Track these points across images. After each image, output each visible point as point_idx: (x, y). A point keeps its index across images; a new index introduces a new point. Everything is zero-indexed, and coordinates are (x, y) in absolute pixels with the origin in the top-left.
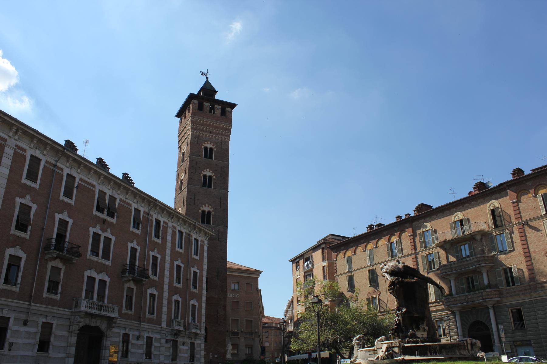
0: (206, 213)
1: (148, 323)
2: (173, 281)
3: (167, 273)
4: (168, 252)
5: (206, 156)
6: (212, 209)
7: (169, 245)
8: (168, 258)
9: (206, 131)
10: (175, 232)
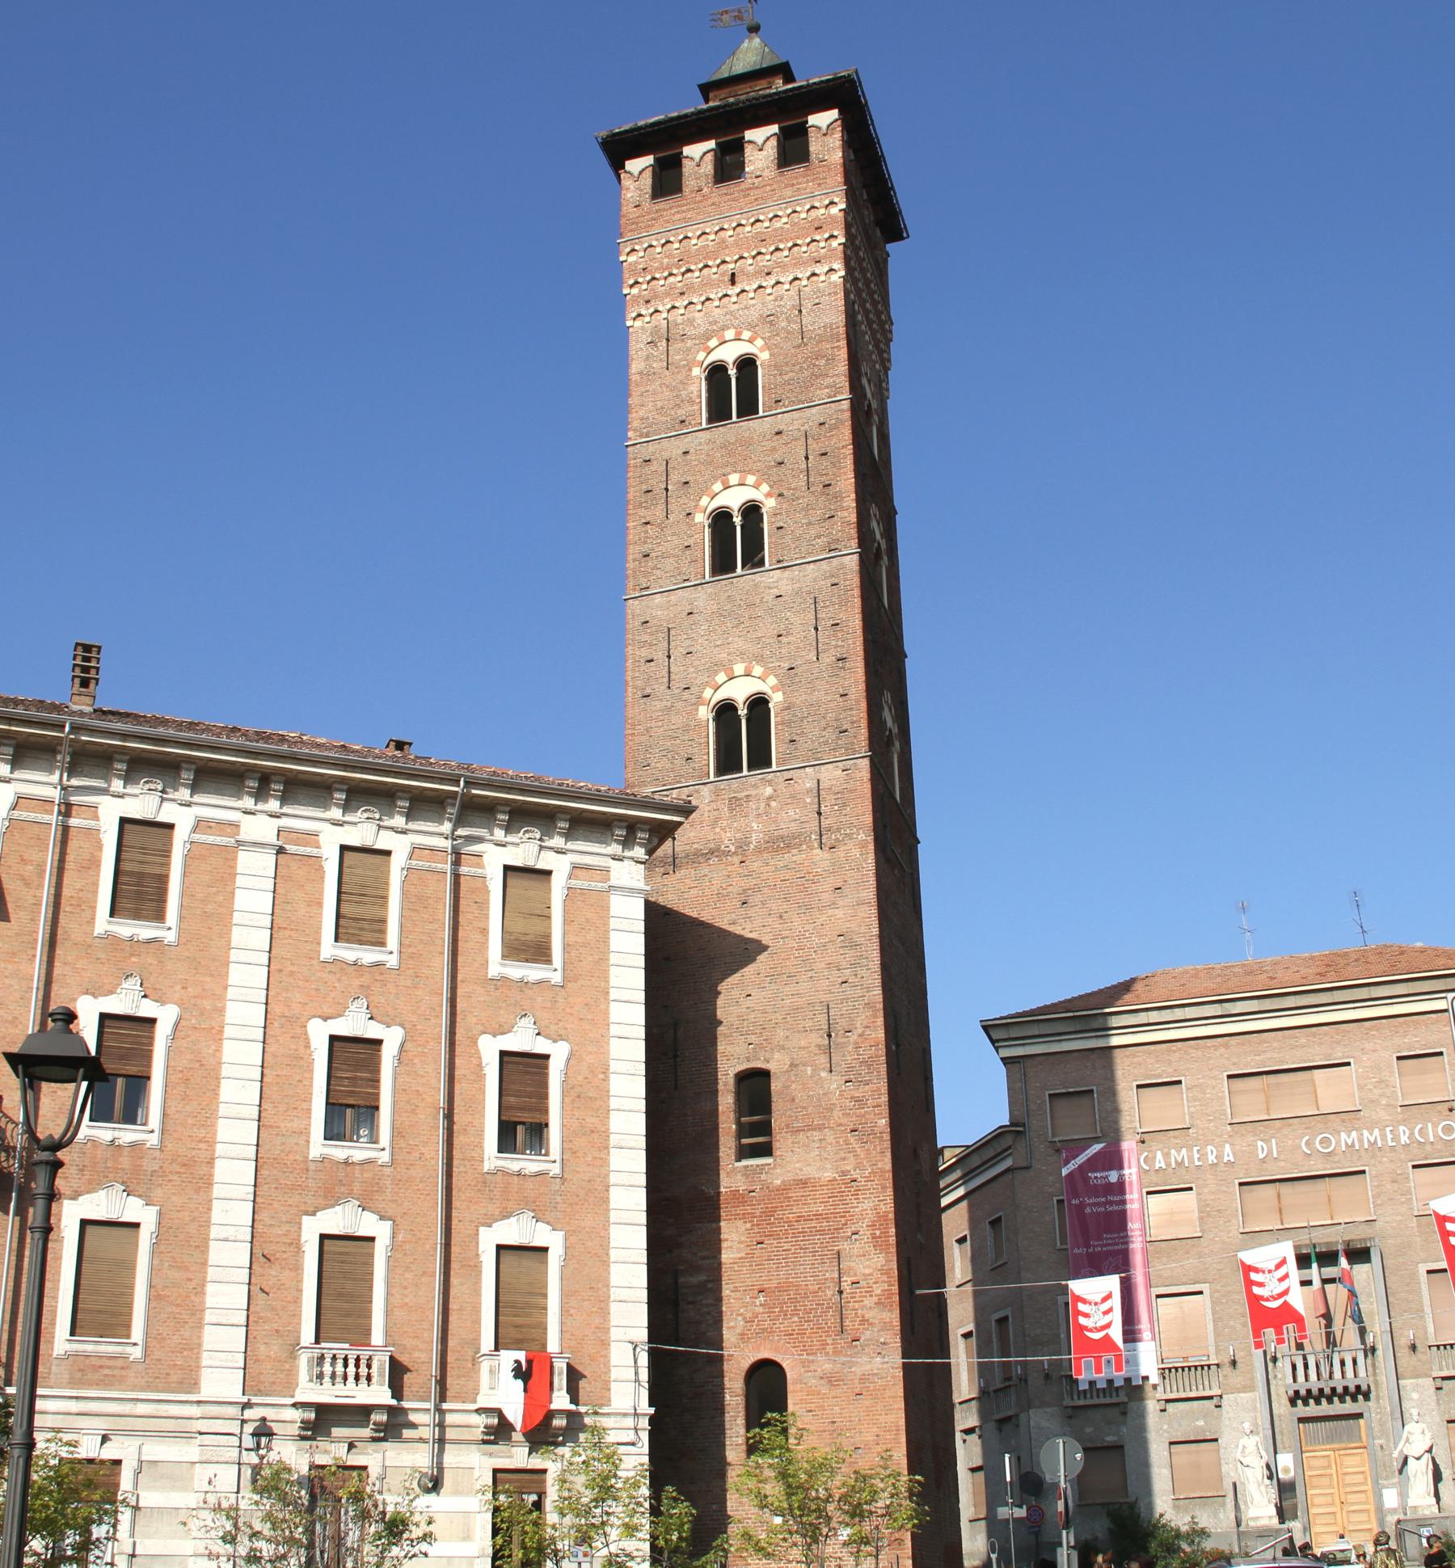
0: (743, 712)
1: (73, 1383)
2: (306, 1132)
3: (238, 1092)
4: (246, 977)
5: (718, 412)
8: (243, 1014)
9: (707, 284)
10: (314, 862)
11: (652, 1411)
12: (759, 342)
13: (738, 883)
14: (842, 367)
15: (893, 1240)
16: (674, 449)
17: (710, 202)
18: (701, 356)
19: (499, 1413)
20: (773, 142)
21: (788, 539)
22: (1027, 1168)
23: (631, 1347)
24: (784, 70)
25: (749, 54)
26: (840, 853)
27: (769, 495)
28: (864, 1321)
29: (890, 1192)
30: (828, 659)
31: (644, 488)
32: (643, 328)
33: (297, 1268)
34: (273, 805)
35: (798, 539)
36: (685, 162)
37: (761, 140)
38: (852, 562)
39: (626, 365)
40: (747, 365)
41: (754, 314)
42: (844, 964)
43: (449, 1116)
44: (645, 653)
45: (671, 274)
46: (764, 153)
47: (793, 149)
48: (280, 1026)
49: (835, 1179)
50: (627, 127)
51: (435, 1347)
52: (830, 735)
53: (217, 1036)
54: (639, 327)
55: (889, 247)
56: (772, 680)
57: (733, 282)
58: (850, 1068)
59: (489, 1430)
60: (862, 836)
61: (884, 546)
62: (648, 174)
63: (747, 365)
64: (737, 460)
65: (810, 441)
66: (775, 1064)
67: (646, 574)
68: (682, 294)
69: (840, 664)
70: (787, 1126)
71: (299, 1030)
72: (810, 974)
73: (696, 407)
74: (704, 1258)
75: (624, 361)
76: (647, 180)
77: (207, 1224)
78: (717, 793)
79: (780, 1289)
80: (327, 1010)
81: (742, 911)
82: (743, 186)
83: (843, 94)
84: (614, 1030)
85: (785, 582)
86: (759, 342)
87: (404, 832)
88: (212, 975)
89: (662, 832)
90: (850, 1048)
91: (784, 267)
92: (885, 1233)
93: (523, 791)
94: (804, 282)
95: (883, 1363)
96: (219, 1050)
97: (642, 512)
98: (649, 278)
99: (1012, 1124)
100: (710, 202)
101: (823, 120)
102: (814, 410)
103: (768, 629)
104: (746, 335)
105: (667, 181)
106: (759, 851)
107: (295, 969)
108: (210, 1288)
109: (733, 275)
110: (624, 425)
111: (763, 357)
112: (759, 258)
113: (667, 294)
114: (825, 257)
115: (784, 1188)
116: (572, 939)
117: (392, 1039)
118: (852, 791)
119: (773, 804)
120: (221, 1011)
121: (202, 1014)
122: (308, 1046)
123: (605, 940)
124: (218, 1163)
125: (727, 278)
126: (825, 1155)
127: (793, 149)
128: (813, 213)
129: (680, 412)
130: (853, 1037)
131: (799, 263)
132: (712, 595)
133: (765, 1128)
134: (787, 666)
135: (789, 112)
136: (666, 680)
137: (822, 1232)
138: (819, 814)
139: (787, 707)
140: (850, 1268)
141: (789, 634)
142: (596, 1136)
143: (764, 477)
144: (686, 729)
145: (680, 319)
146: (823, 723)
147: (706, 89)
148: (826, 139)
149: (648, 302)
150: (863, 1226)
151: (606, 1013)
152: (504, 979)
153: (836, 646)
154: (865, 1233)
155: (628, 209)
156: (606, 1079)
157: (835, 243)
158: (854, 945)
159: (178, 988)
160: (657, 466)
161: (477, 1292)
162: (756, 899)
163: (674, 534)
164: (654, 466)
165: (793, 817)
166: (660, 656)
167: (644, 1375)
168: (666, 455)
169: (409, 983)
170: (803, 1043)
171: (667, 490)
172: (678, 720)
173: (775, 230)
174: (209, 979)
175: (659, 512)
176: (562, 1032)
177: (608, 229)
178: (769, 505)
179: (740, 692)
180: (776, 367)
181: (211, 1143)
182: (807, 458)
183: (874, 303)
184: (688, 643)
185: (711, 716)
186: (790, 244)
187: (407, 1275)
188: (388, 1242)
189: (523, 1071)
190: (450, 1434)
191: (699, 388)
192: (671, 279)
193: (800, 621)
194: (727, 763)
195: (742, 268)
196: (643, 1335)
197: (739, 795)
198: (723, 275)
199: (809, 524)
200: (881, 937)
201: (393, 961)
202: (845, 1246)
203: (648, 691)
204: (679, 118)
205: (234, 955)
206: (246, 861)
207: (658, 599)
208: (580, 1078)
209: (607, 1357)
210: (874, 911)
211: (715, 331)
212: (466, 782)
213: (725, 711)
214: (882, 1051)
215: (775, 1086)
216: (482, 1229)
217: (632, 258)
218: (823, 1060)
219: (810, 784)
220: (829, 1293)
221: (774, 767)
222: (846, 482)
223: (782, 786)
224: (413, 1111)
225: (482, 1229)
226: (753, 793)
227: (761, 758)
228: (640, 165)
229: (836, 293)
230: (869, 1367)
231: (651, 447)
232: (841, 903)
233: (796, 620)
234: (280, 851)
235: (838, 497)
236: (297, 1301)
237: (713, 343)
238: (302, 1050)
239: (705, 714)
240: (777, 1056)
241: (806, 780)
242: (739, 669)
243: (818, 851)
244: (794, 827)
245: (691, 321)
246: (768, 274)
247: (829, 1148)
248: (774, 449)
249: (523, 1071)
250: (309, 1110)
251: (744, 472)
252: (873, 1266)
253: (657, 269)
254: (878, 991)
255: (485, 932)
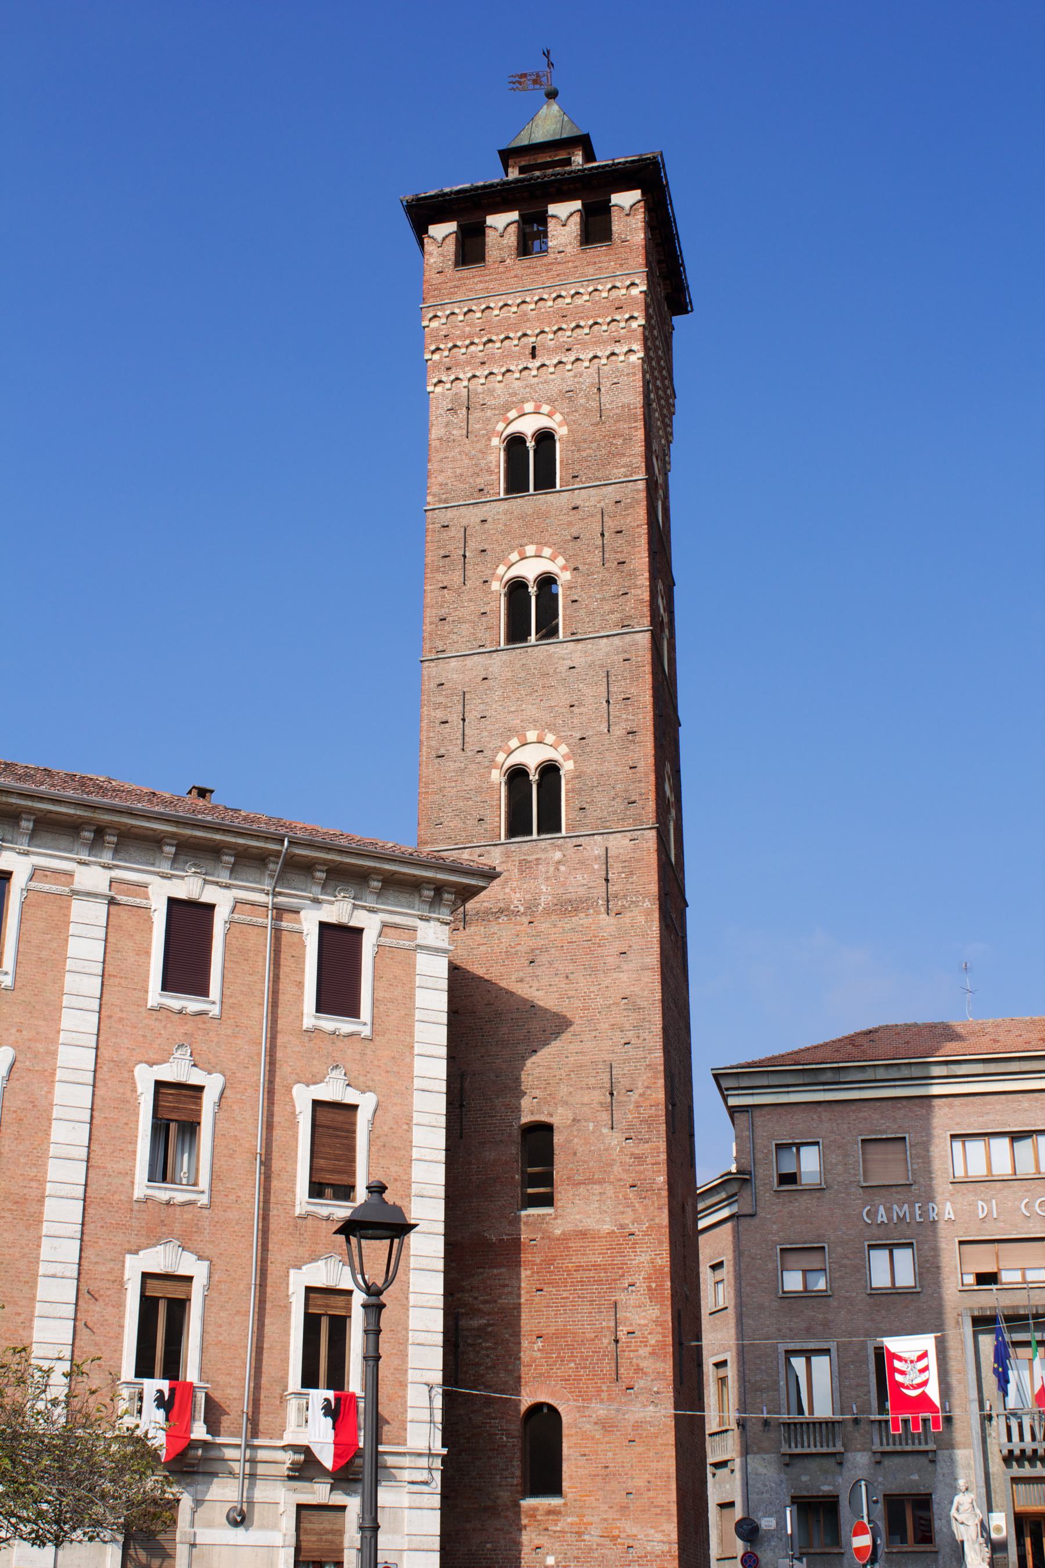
0: (534, 777)
2: (130, 1173)
3: (68, 1134)
4: (78, 1023)
5: (516, 484)
6: (564, 749)
7: (81, 985)
8: (75, 1058)
9: (508, 356)
11: (445, 1451)
12: (558, 417)
13: (526, 944)
14: (639, 448)
15: (668, 1293)
16: (472, 516)
17: (513, 273)
18: (500, 426)
19: (307, 1450)
20: (576, 219)
21: (582, 612)
22: (752, 1216)
23: (426, 1388)
24: (583, 142)
25: (547, 123)
26: (626, 919)
27: (564, 568)
28: (638, 1370)
29: (666, 1246)
30: (618, 731)
31: (442, 553)
32: (443, 394)
33: (120, 1305)
34: (107, 858)
35: (592, 613)
36: (488, 231)
37: (565, 215)
38: (644, 640)
39: (426, 429)
40: (545, 438)
41: (553, 390)
42: (627, 1026)
43: (266, 1163)
44: (440, 715)
45: (472, 343)
46: (567, 228)
47: (596, 228)
48: (107, 1071)
49: (613, 1232)
50: (432, 193)
51: (247, 1385)
52: (619, 805)
53: (49, 1078)
54: (440, 394)
55: (677, 320)
56: (564, 749)
57: (533, 355)
58: (630, 1127)
59: (295, 1467)
60: (647, 904)
61: (666, 620)
62: (452, 240)
63: (545, 438)
64: (534, 532)
65: (606, 519)
66: (558, 1118)
67: (442, 638)
68: (483, 363)
69: (630, 737)
70: (569, 1179)
71: (126, 1075)
72: (594, 1033)
73: (494, 477)
74: (486, 1302)
75: (425, 427)
76: (451, 246)
77: (37, 1260)
78: (507, 855)
79: (557, 1335)
80: (152, 1056)
81: (530, 969)
82: (545, 260)
83: (647, 176)
84: (417, 1083)
85: (578, 654)
86: (558, 417)
87: (227, 887)
88: (45, 1019)
89: (467, 893)
90: (631, 1107)
91: (584, 345)
92: (660, 1286)
93: (341, 851)
94: (604, 361)
95: (659, 1412)
96: (51, 1092)
97: (440, 576)
98: (450, 345)
99: (739, 1172)
100: (513, 273)
101: (626, 199)
102: (610, 488)
103: (560, 698)
104: (545, 409)
105: (470, 250)
106: (547, 912)
107: (124, 1015)
108: (37, 1323)
109: (534, 348)
110: (423, 489)
111: (561, 432)
112: (560, 333)
113: (468, 363)
114: (625, 338)
115: (565, 1238)
116: (380, 994)
117: (213, 1085)
118: (638, 860)
119: (562, 868)
120: (54, 1054)
121: (35, 1057)
122: (134, 1090)
123: (412, 997)
124: (48, 1202)
125: (528, 351)
126: (605, 1208)
127: (596, 228)
128: (614, 292)
129: (479, 480)
130: (635, 1096)
131: (599, 342)
132: (505, 662)
133: (547, 1179)
134: (579, 735)
135: (594, 191)
136: (460, 742)
137: (599, 1282)
138: (607, 880)
139: (578, 776)
140: (626, 1318)
141: (581, 705)
142: (399, 1184)
143: (560, 550)
144: (479, 791)
145: (480, 389)
146: (613, 793)
147: (507, 156)
148: (629, 219)
149: (448, 369)
150: (639, 1279)
151: (411, 1066)
152: (317, 1030)
153: (627, 720)
154: (642, 1286)
155: (431, 275)
156: (409, 1130)
157: (634, 324)
158: (638, 1009)
159: (13, 1030)
160: (456, 532)
161: (287, 1332)
162: (544, 958)
163: (470, 600)
164: (452, 531)
165: (582, 882)
166: (455, 719)
167: (438, 1416)
168: (464, 522)
169: (229, 1032)
170: (586, 1100)
171: (464, 556)
172: (471, 782)
173: (576, 307)
174: (43, 1023)
175: (456, 577)
176: (370, 1083)
177: (413, 297)
178: (564, 577)
179: (531, 758)
180: (573, 441)
181: (42, 1182)
182: (602, 535)
183: (663, 378)
184: (482, 707)
185: (503, 779)
186: (591, 322)
187: (222, 1314)
188: (205, 1282)
189: (333, 1121)
190: (261, 1469)
191: (499, 459)
192: (473, 348)
193: (593, 693)
194: (518, 826)
195: (542, 339)
196: (438, 1377)
197: (529, 858)
198: (524, 347)
199: (603, 599)
200: (663, 1001)
201: (215, 1010)
202: (621, 1297)
203: (442, 751)
204: (484, 187)
205: (66, 1000)
206: (78, 907)
207: (453, 663)
208: (386, 1128)
209: (404, 1397)
210: (657, 977)
211: (514, 402)
212: (289, 842)
213: (517, 775)
214: (662, 1112)
215: (558, 1139)
216: (292, 1272)
217: (434, 324)
218: (605, 1116)
219: (599, 851)
220: (605, 1341)
221: (564, 833)
222: (640, 560)
223: (571, 851)
224: (231, 1156)
225: (292, 1272)
226: (543, 856)
227: (550, 823)
228: (443, 231)
229: (634, 374)
230: (642, 1415)
231: (450, 513)
232: (625, 967)
233: (589, 692)
234: (112, 902)
235: (632, 574)
236: (119, 1337)
237: (512, 414)
238: (129, 1094)
239: (498, 777)
240: (560, 1110)
241: (595, 847)
242: (532, 735)
243: (605, 916)
244: (582, 891)
245: (491, 392)
246: (568, 350)
247: (609, 1202)
248: (570, 524)
249: (333, 1121)
250: (134, 1152)
251: (541, 544)
252: (648, 1316)
253: (459, 337)
254: (659, 1054)
255: (300, 985)
